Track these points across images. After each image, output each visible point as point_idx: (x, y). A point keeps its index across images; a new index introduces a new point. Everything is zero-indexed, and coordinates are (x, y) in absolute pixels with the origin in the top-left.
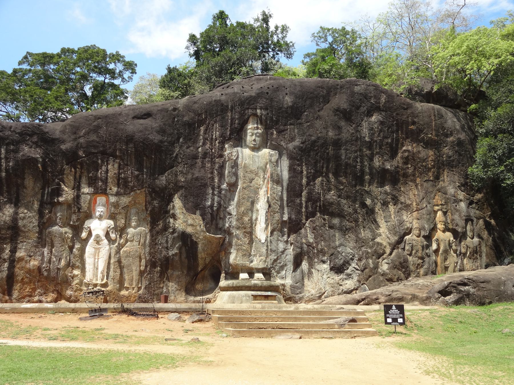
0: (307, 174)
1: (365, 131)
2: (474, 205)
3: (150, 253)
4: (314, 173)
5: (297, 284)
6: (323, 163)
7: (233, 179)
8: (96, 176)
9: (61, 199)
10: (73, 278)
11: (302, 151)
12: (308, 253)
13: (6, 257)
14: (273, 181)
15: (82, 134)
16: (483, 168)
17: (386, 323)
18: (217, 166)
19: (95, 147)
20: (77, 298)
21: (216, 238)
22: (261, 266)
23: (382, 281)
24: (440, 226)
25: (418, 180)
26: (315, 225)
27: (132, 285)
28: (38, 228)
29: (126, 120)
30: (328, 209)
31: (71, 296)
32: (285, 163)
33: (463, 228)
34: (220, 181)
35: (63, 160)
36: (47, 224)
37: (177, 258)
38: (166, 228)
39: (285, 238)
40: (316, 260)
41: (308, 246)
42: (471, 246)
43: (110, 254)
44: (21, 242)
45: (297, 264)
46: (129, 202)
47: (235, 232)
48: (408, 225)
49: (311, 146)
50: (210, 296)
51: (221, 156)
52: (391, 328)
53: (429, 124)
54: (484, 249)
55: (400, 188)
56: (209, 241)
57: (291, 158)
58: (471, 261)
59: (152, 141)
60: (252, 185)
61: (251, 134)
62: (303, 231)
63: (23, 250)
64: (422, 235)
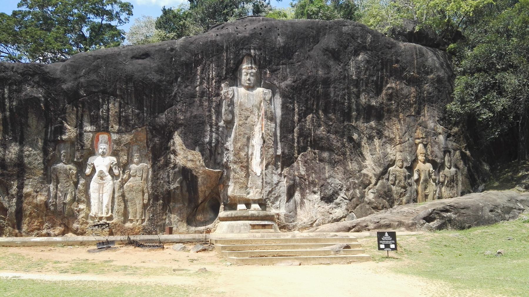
0: (299, 111)
1: (352, 70)
2: (451, 138)
3: (152, 188)
4: (305, 110)
5: (291, 214)
6: (313, 101)
7: (230, 117)
8: (98, 115)
9: (64, 137)
10: (78, 212)
11: (294, 90)
12: (300, 184)
13: (14, 193)
14: (267, 118)
15: (82, 74)
16: (461, 104)
17: (380, 249)
18: (214, 104)
19: (96, 86)
20: (83, 231)
21: (215, 172)
22: (257, 197)
23: (368, 209)
24: (421, 158)
25: (401, 115)
26: (306, 159)
27: (136, 217)
28: (43, 165)
29: (125, 60)
30: (318, 144)
31: (77, 229)
32: (278, 101)
33: (442, 159)
34: (217, 118)
35: (64, 99)
36: (52, 161)
37: (178, 192)
38: (167, 163)
39: (279, 171)
40: (308, 191)
41: (300, 178)
42: (449, 175)
43: (114, 189)
44: (27, 178)
45: (290, 195)
46: (131, 140)
47: (232, 166)
48: (392, 157)
49: (302, 84)
50: (210, 226)
51: (218, 95)
52: (384, 253)
53: (411, 62)
54: (460, 178)
55: (384, 123)
56: (208, 175)
57: (284, 96)
58: (448, 189)
59: (151, 80)
60: (247, 122)
61: (245, 73)
62: (295, 164)
63: (30, 186)
64: (404, 166)
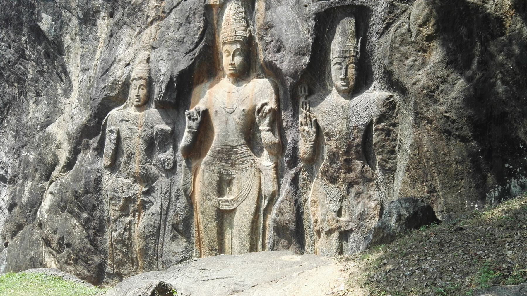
54: (406, 134)
